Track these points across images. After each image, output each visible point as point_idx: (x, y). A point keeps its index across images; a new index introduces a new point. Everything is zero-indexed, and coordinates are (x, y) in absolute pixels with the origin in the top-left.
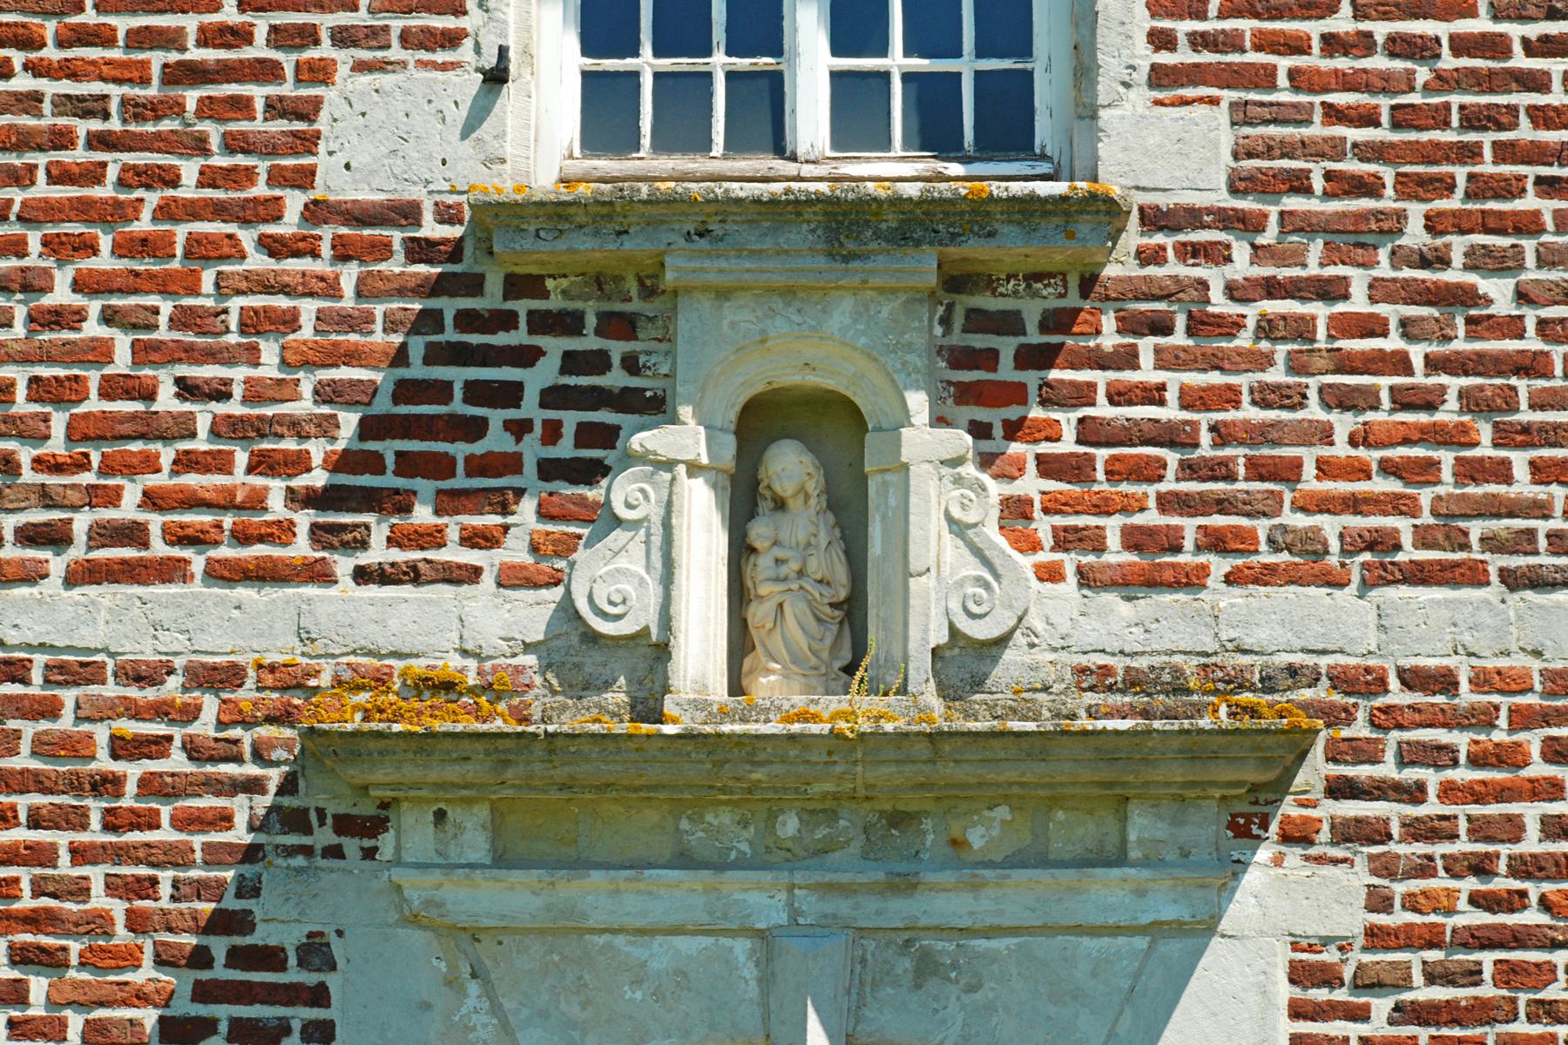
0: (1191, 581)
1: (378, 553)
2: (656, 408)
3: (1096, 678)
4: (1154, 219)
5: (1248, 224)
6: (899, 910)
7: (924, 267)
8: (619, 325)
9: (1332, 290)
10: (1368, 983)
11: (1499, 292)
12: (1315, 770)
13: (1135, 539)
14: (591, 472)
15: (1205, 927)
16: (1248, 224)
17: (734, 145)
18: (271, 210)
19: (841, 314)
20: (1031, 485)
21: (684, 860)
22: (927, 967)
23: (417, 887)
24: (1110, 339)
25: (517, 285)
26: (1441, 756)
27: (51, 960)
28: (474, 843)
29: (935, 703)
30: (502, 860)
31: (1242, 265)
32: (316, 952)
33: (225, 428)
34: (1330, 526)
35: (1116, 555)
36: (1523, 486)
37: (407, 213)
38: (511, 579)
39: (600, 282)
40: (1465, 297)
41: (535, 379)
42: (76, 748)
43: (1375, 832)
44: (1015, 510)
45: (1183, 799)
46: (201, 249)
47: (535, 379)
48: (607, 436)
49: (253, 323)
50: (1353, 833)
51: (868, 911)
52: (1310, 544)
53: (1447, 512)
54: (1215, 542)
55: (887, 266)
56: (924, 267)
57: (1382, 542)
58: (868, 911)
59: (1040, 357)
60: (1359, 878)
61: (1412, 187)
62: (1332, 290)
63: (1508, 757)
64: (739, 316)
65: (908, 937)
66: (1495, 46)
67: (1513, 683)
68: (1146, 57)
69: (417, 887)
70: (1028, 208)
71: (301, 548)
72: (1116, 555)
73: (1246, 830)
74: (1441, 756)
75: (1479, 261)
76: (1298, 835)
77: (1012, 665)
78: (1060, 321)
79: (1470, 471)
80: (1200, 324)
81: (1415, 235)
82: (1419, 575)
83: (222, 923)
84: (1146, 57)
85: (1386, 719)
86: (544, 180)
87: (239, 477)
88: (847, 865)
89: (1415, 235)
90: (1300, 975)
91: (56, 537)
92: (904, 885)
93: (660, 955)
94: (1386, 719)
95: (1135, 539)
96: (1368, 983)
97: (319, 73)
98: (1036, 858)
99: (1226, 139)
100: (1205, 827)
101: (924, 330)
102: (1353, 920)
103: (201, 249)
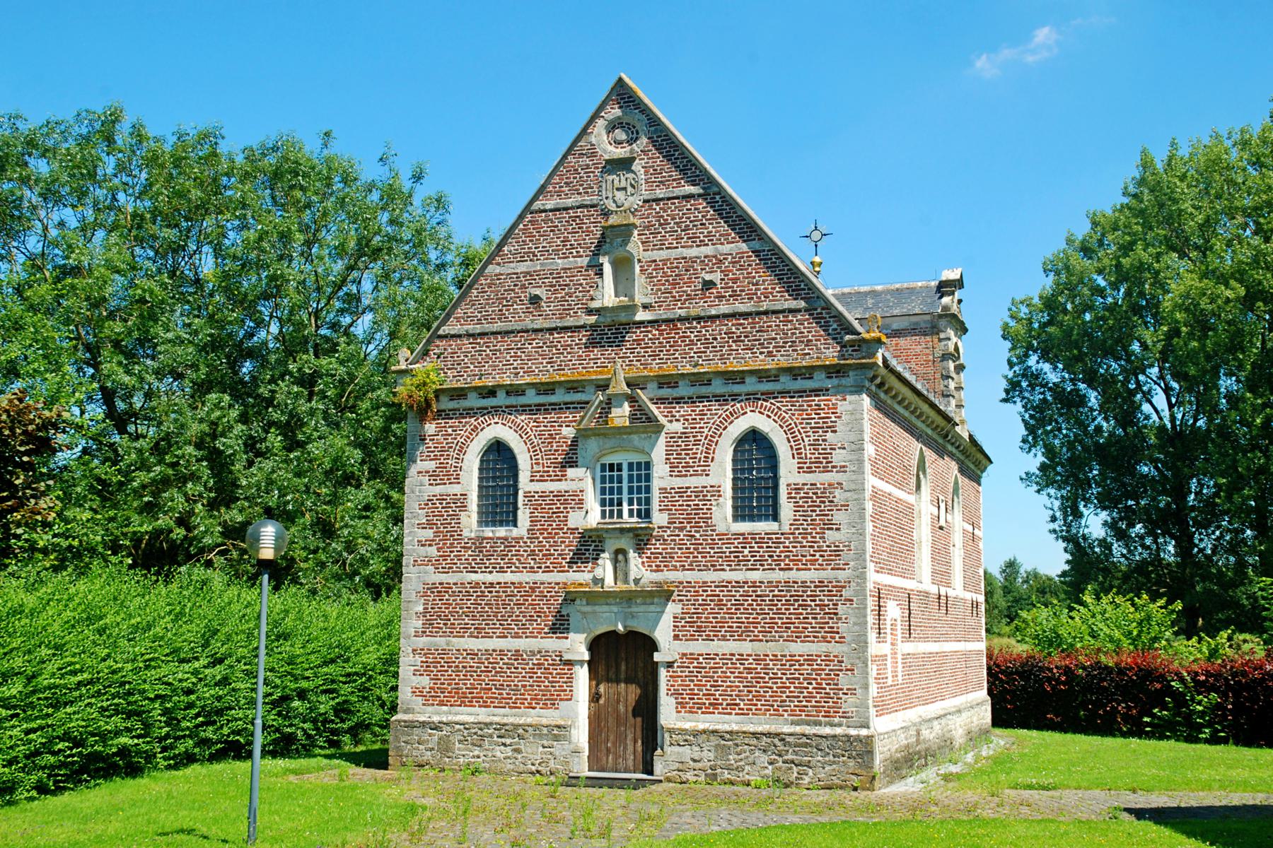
0: (662, 571)
1: (575, 569)
2: (603, 551)
3: (652, 582)
4: (659, 527)
5: (669, 528)
6: (629, 610)
7: (631, 535)
8: (600, 542)
9: (679, 535)
10: (682, 618)
11: (698, 535)
12: (676, 593)
13: (656, 566)
14: (597, 559)
15: (663, 612)
16: (669, 528)
17: (618, 517)
18: (563, 529)
19: (623, 540)
20: (645, 560)
21: (607, 604)
22: (633, 617)
23: (578, 608)
24: (654, 542)
25: (590, 537)
26: (690, 591)
27: (540, 616)
28: (584, 602)
29: (633, 585)
30: (588, 604)
31: (669, 533)
32: (568, 615)
33: (559, 555)
34: (678, 564)
35: (654, 568)
36: (700, 559)
37: (577, 529)
38: (589, 571)
39: (598, 536)
40: (694, 536)
41: (592, 548)
42: (542, 592)
43: (681, 601)
44: (643, 563)
45: (660, 597)
46: (556, 534)
47: (592, 548)
48: (598, 555)
49: (562, 542)
50: (681, 601)
51: (627, 610)
52: (675, 566)
53: (692, 562)
54: (665, 566)
55: (627, 535)
56: (631, 535)
57: (684, 566)
58: (627, 610)
59: (646, 544)
60: (681, 606)
61: (688, 523)
62: (679, 535)
63: (697, 591)
64: (612, 541)
65: (631, 613)
66: (698, 505)
67: (698, 583)
68: (658, 508)
69: (578, 608)
70: (641, 528)
71: (566, 568)
72: (654, 568)
73: (668, 600)
74: (690, 591)
75: (696, 531)
76: (674, 601)
77: (642, 581)
78: (648, 540)
79: (694, 557)
80: (664, 540)
81: (688, 529)
82: (688, 570)
83: (558, 612)
84: (658, 508)
85: (684, 587)
86: (594, 526)
87: (560, 560)
88: (624, 605)
89: (688, 529)
90: (674, 617)
91: (540, 568)
92: (630, 607)
93: (604, 615)
94: (684, 587)
95: (656, 566)
96: (682, 618)
97: (568, 512)
98: (645, 604)
99: (667, 517)
100: (663, 600)
101: (633, 542)
102: (680, 611)
103: (556, 534)
